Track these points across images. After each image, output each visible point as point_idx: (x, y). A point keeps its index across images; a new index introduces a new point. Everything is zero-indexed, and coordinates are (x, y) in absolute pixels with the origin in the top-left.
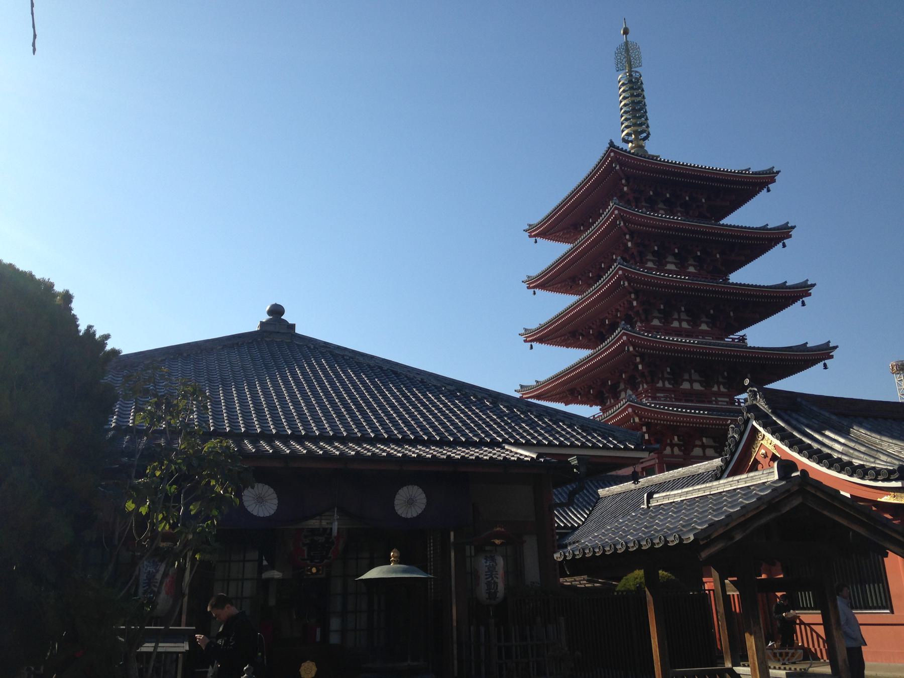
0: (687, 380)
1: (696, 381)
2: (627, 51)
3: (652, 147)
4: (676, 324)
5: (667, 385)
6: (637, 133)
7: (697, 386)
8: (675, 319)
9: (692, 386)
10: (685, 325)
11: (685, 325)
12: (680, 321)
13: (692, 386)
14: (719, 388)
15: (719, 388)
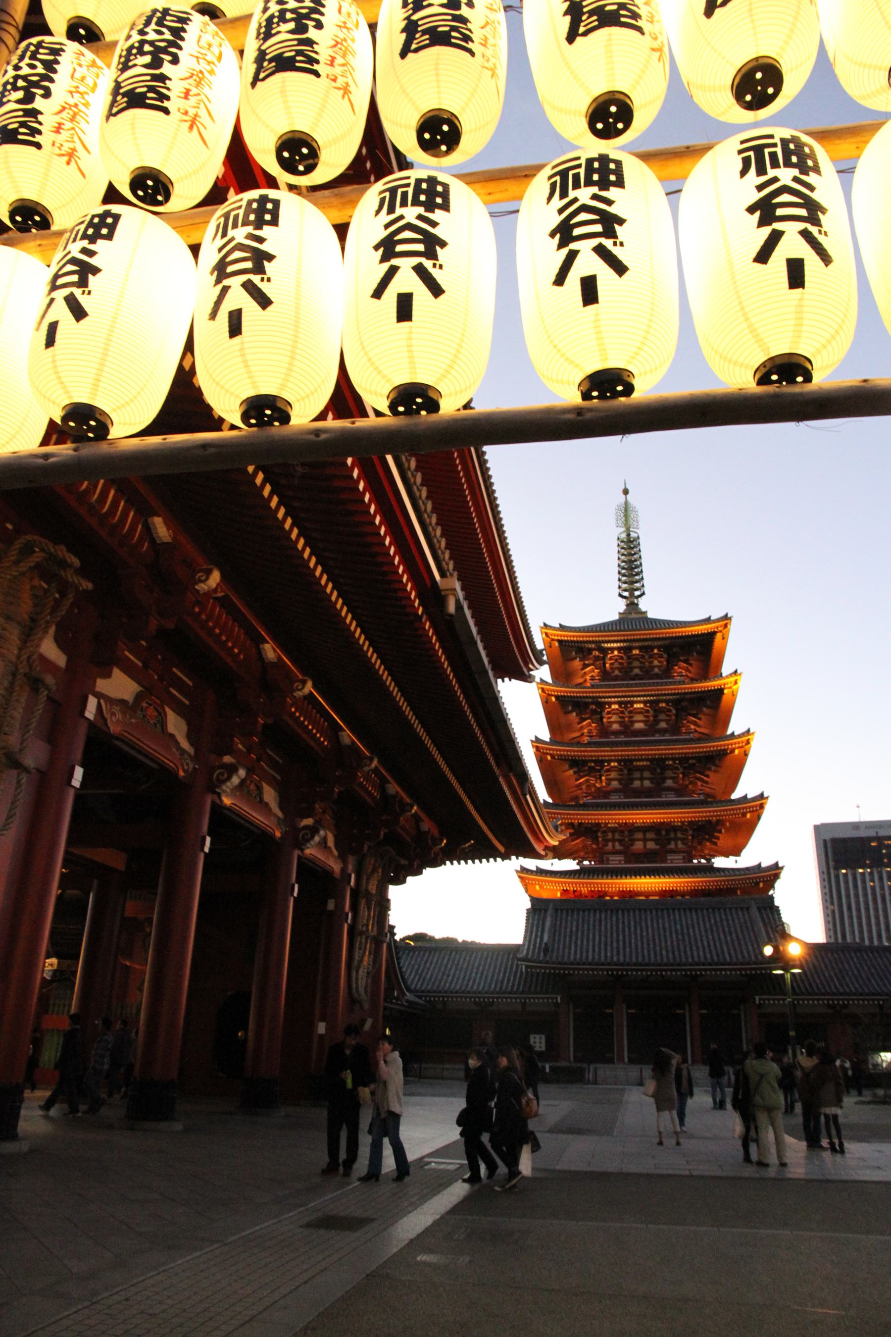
0: (639, 840)
1: (651, 840)
2: (626, 510)
3: (644, 604)
4: (637, 783)
5: (618, 846)
6: (631, 591)
7: (651, 845)
8: (637, 779)
9: (645, 846)
10: (647, 783)
11: (647, 783)
12: (642, 779)
13: (645, 846)
14: (676, 845)
15: (676, 845)
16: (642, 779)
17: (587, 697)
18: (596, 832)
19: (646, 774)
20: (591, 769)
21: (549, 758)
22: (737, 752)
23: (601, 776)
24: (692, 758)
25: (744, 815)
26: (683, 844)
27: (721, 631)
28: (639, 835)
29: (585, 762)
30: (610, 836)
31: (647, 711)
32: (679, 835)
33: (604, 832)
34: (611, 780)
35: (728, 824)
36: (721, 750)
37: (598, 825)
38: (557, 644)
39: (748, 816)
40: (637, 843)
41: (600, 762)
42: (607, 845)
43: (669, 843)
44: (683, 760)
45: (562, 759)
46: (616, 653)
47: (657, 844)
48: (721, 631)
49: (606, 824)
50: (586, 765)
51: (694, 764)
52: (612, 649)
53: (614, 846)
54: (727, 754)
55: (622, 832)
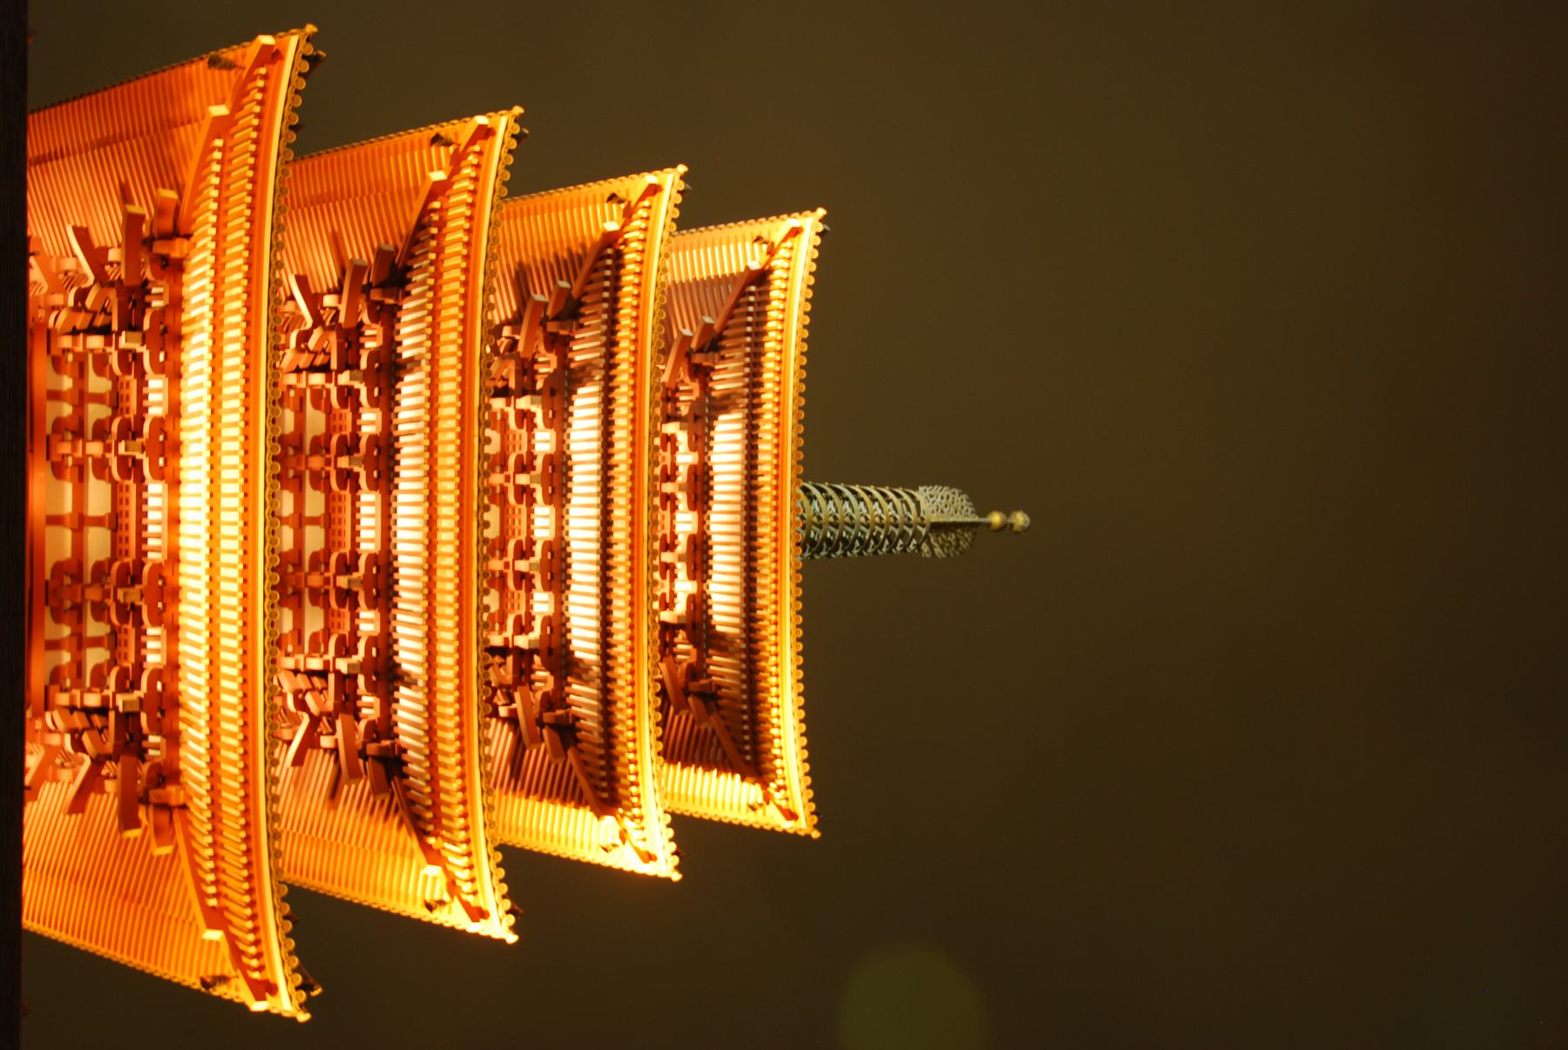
8: (299, 503)
12: (300, 521)
16: (300, 521)
17: (611, 344)
18: (131, 325)
19: (314, 539)
20: (351, 338)
21: (438, 176)
22: (435, 871)
23: (325, 369)
24: (388, 701)
25: (216, 918)
26: (56, 676)
27: (767, 798)
28: (98, 498)
29: (388, 316)
30: (98, 384)
31: (524, 552)
32: (95, 657)
33: (130, 361)
34: (300, 410)
35: (166, 850)
36: (436, 806)
37: (169, 337)
38: (755, 265)
39: (216, 935)
40: (68, 488)
41: (388, 370)
42: (58, 364)
43: (58, 619)
44: (387, 675)
45: (421, 226)
46: (686, 458)
47: (59, 567)
48: (767, 798)
49: (175, 375)
50: (375, 318)
51: (356, 715)
52: (701, 442)
53: (56, 395)
54: (422, 834)
55: (131, 431)
